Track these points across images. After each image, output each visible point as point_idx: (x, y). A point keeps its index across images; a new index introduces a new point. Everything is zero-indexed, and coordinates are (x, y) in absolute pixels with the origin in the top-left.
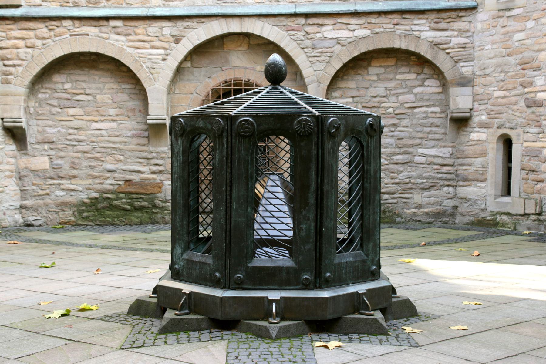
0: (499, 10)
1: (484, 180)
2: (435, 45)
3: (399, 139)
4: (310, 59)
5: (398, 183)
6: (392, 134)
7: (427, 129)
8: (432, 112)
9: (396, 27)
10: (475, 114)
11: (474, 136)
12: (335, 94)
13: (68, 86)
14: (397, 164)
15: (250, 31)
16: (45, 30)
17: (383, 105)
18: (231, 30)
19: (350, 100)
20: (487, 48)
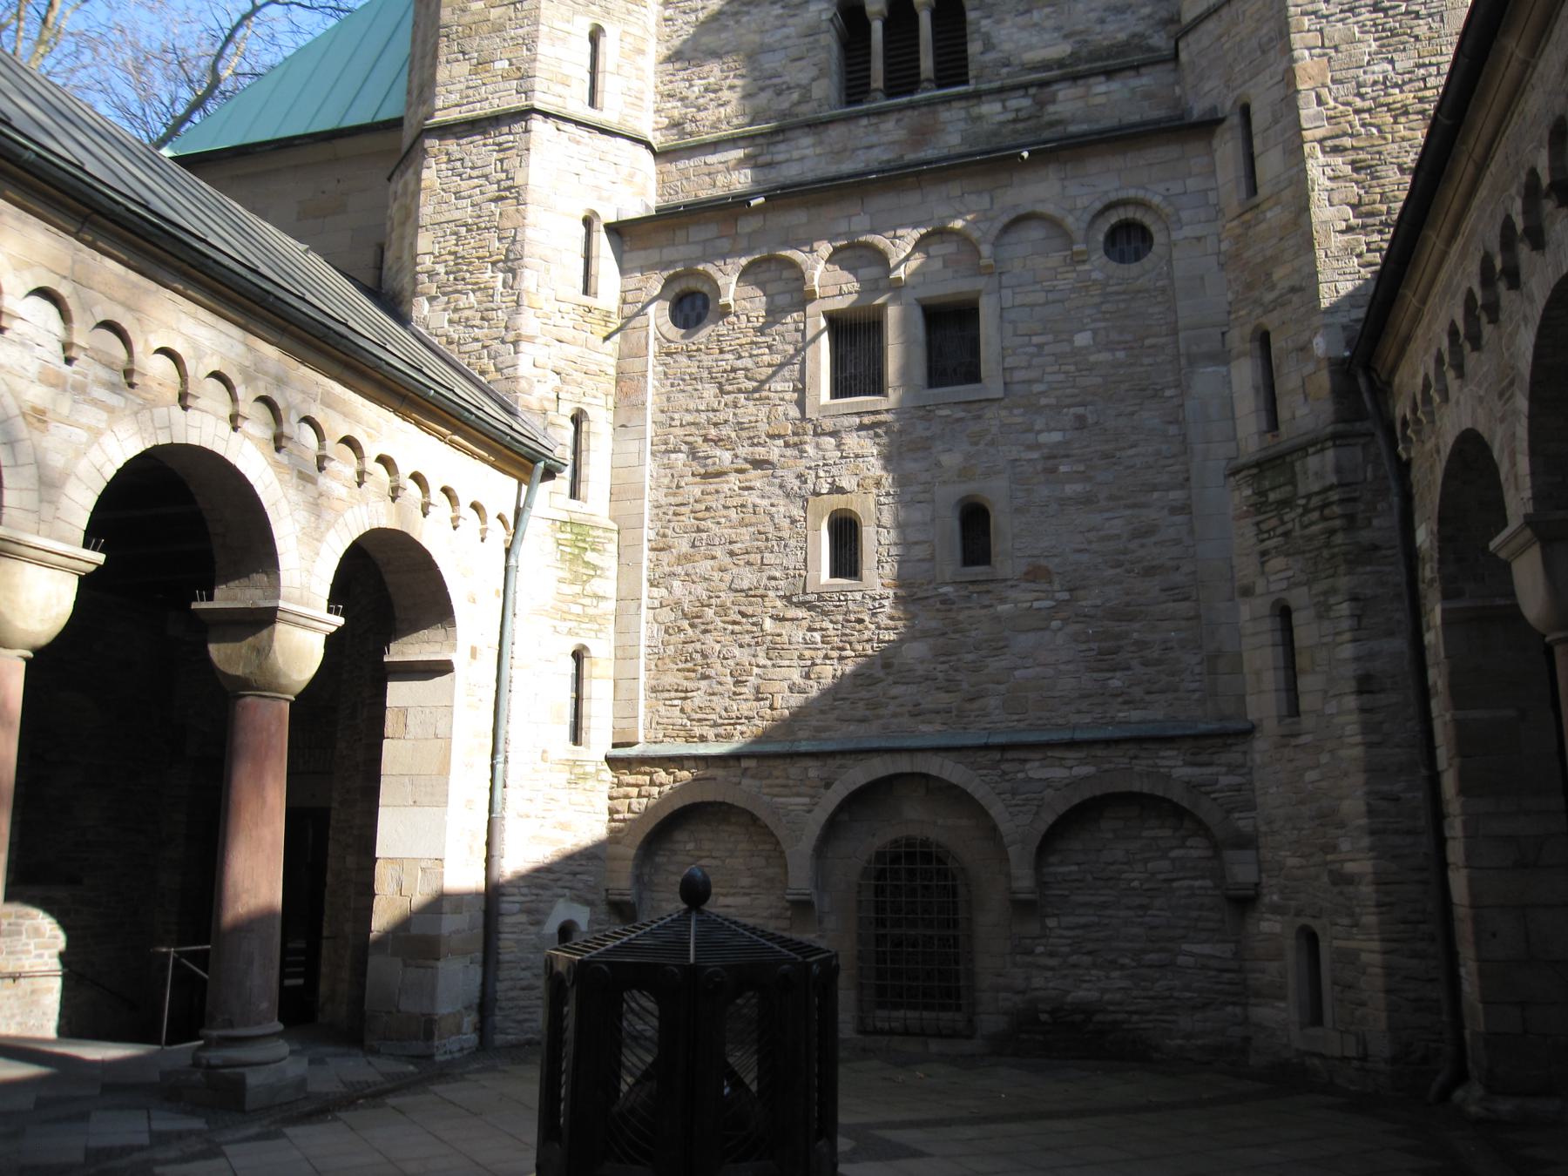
0: (1283, 736)
1: (1283, 998)
2: (1194, 787)
3: (1152, 928)
4: (1011, 809)
5: (1152, 998)
6: (1140, 920)
7: (1194, 914)
8: (1201, 888)
9: (1134, 761)
10: (1265, 891)
11: (1265, 926)
12: (1053, 859)
13: (690, 846)
14: (1150, 966)
15: (924, 771)
16: (663, 774)
17: (1124, 876)
18: (899, 770)
19: (1074, 868)
20: (1271, 791)
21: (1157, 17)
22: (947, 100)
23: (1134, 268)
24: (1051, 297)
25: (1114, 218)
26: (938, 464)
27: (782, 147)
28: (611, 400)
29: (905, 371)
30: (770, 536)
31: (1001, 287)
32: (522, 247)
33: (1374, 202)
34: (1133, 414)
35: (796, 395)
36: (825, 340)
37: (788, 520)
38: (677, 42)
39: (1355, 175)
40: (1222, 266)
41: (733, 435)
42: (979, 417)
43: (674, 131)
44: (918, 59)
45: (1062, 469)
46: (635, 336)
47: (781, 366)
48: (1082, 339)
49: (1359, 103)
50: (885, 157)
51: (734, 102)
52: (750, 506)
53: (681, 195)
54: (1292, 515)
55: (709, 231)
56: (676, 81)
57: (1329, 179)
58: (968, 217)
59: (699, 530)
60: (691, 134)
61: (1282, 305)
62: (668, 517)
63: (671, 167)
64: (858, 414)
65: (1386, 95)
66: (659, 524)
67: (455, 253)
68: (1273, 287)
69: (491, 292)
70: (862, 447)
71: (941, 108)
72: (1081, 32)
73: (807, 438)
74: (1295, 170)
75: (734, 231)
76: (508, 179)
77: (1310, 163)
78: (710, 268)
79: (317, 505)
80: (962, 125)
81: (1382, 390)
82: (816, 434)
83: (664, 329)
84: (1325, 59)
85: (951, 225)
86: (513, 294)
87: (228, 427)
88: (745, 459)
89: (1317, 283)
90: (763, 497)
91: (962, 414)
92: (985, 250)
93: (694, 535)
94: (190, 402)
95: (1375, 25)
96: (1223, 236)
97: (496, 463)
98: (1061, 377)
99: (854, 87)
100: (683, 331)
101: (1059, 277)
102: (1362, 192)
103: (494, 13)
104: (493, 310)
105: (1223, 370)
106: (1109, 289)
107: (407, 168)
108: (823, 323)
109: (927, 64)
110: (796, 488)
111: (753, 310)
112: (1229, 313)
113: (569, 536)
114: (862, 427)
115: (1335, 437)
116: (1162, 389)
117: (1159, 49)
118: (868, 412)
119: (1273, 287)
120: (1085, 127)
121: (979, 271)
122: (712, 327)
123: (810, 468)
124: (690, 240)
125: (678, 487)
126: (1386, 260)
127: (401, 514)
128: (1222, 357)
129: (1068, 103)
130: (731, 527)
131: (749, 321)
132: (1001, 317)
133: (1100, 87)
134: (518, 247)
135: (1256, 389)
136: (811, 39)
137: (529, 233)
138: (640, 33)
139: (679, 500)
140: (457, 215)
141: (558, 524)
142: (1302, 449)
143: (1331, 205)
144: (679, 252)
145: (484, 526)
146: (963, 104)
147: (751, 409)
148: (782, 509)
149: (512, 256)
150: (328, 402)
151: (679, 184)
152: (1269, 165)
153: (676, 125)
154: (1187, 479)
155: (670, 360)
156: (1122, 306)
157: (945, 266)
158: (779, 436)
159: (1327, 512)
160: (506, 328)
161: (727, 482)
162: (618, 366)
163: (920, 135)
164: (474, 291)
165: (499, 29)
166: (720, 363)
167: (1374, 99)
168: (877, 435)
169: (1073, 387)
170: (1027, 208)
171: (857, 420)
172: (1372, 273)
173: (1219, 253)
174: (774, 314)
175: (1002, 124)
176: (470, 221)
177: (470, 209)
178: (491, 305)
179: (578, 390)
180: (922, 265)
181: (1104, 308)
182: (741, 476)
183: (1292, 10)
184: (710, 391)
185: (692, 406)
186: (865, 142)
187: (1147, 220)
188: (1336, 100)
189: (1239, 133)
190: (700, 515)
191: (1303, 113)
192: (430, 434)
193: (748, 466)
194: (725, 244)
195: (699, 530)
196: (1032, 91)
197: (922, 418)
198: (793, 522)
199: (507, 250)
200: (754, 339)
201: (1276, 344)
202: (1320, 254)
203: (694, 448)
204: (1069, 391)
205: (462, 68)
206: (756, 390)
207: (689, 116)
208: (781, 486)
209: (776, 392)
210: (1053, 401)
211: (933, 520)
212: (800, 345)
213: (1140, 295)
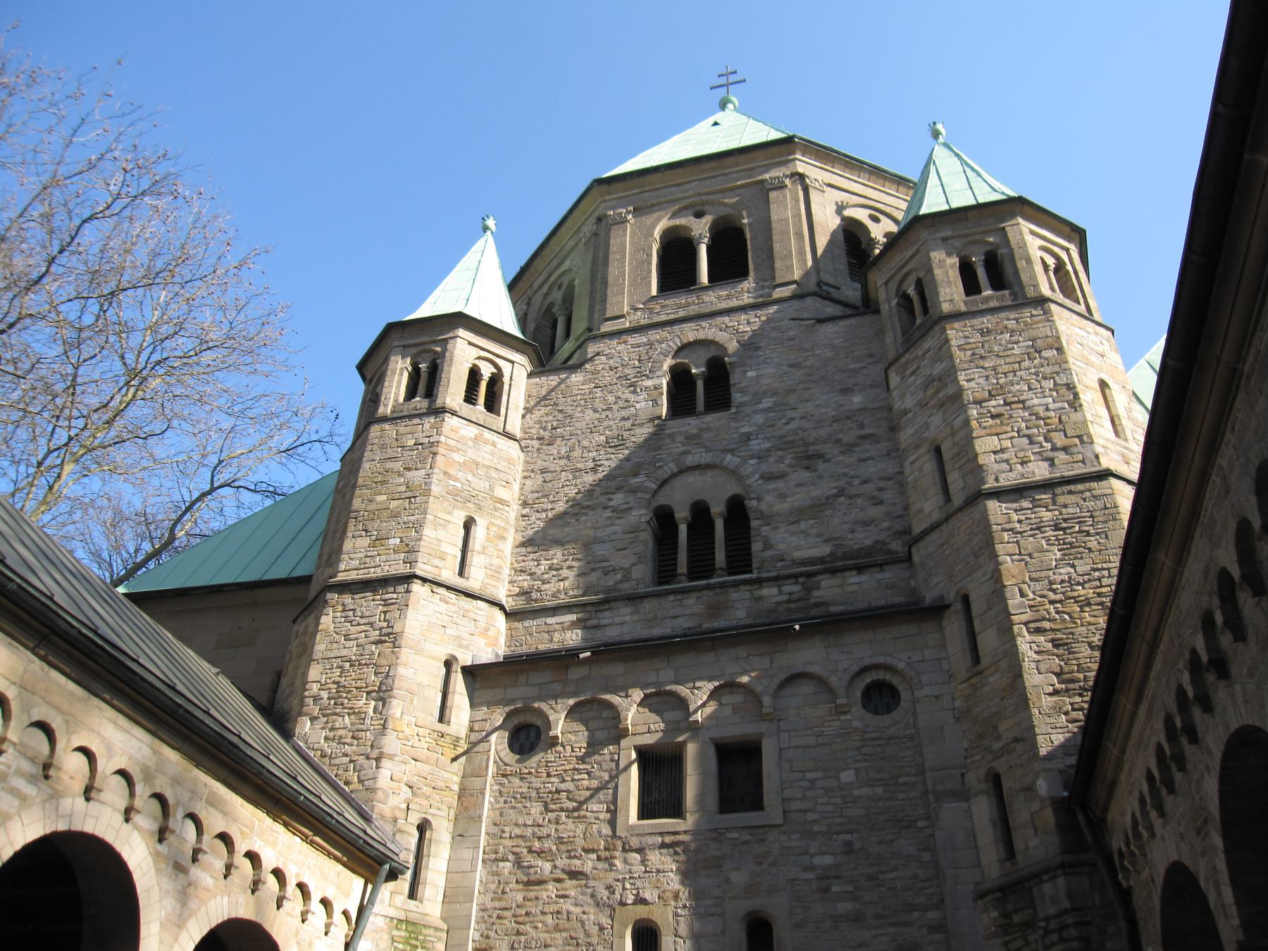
22: (736, 584)
23: (887, 719)
24: (820, 740)
25: (868, 678)
26: (728, 881)
27: (607, 614)
29: (701, 799)
30: (580, 941)
31: (779, 731)
32: (393, 681)
33: (1073, 672)
34: (892, 841)
35: (609, 815)
36: (634, 769)
37: (597, 928)
38: (530, 532)
39: (1055, 651)
40: (957, 719)
41: (554, 848)
42: (762, 840)
43: (523, 598)
44: (714, 553)
45: (835, 888)
46: (478, 759)
47: (598, 790)
48: (847, 776)
49: (1052, 596)
50: (687, 625)
51: (571, 579)
52: (565, 912)
53: (524, 647)
54: (1036, 936)
55: (546, 676)
58: (753, 674)
59: (518, 933)
60: (536, 601)
61: (1008, 752)
62: (492, 920)
63: (519, 625)
64: (661, 834)
65: (1072, 590)
66: (484, 926)
67: (338, 683)
68: (999, 738)
69: (363, 715)
70: (663, 863)
71: (731, 590)
72: (836, 539)
73: (617, 854)
74: (1008, 646)
76: (388, 627)
77: (1019, 641)
78: (544, 706)
79: (185, 894)
80: (747, 603)
81: (1099, 826)
82: (624, 850)
83: (502, 754)
84: (1023, 563)
85: (739, 680)
86: (381, 719)
87: (121, 818)
88: (563, 870)
89: (1035, 735)
90: (576, 905)
91: (747, 837)
92: (767, 700)
93: (514, 937)
94: (93, 794)
95: (1057, 540)
96: (956, 696)
97: (349, 864)
98: (831, 808)
99: (664, 571)
100: (518, 757)
101: (826, 724)
102: (1062, 663)
103: (394, 504)
105: (965, 805)
106: (867, 736)
107: (309, 615)
108: (634, 755)
109: (720, 557)
110: (605, 898)
111: (577, 742)
112: (966, 758)
113: (403, 934)
114: (663, 846)
115: (1063, 866)
116: (915, 821)
117: (897, 553)
118: (669, 833)
119: (999, 738)
120: (842, 608)
121: (762, 717)
122: (542, 754)
123: (618, 880)
124: (530, 683)
125: (503, 892)
126: (1088, 717)
127: (259, 908)
128: (963, 794)
129: (829, 590)
130: (546, 932)
131: (573, 751)
132: (780, 756)
133: (853, 579)
134: (390, 680)
135: (994, 822)
136: (633, 535)
137: (401, 670)
138: (503, 524)
139: (503, 904)
140: (344, 652)
141: (395, 921)
142: (1037, 876)
144: (520, 692)
145: (329, 921)
146: (749, 587)
147: (571, 826)
148: (592, 917)
149: (384, 688)
150: (213, 802)
152: (988, 641)
153: (524, 593)
154: (942, 901)
156: (878, 749)
157: (734, 713)
158: (593, 851)
159: (1065, 934)
160: (372, 746)
161: (546, 890)
162: (461, 784)
163: (715, 610)
164: (349, 714)
167: (1063, 593)
168: (676, 853)
169: (841, 817)
170: (800, 669)
171: (660, 840)
172: (1077, 727)
173: (953, 709)
174: (594, 746)
175: (778, 603)
176: (354, 658)
177: (355, 648)
178: (362, 726)
179: (426, 803)
180: (715, 711)
181: (864, 750)
182: (558, 885)
184: (536, 809)
185: (520, 821)
186: (673, 613)
187: (895, 681)
188: (1034, 593)
190: (520, 919)
191: (1010, 602)
192: (294, 834)
193: (565, 876)
194: (557, 687)
195: (518, 933)
196: (801, 580)
197: (715, 839)
198: (602, 929)
199: (381, 683)
201: (1007, 785)
202: (1035, 711)
203: (520, 858)
204: (837, 820)
206: (575, 809)
207: (536, 587)
208: (592, 896)
209: (592, 812)
210: (824, 828)
211: (723, 932)
212: (614, 773)
213: (892, 741)
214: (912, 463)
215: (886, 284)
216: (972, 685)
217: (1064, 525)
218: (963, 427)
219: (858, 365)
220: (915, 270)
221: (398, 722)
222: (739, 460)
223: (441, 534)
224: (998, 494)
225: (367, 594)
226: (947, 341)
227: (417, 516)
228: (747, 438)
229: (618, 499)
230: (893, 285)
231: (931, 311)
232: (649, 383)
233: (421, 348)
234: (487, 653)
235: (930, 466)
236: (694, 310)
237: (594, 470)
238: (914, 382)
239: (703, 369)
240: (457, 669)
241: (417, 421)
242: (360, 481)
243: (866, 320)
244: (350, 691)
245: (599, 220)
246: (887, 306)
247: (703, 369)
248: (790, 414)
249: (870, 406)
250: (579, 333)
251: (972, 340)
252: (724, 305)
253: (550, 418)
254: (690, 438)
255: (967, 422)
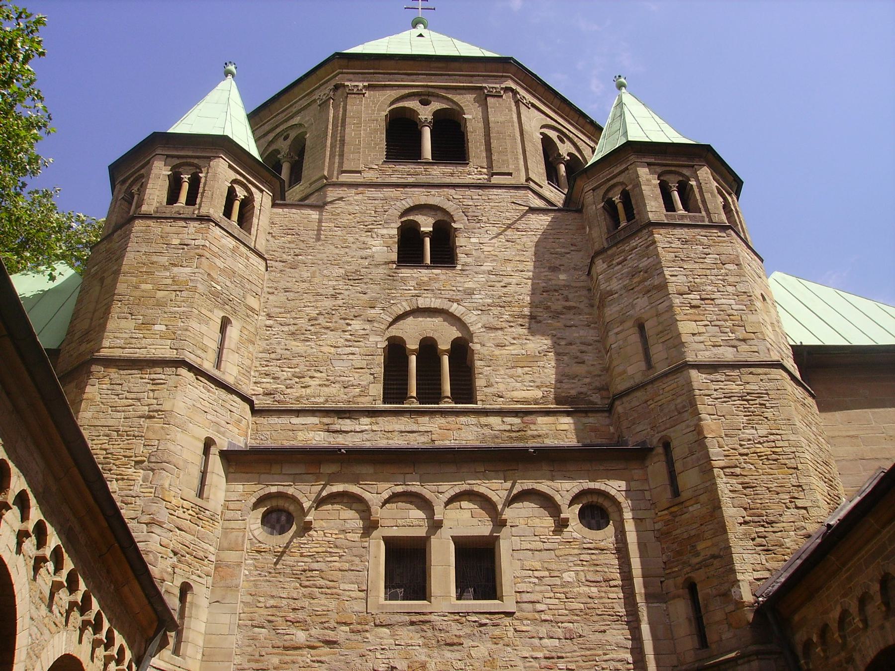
21: (594, 385)
26: (470, 656)
28: (210, 580)
48: (568, 577)
56: (272, 366)
57: (730, 491)
61: (707, 566)
68: (697, 554)
74: (708, 484)
75: (318, 471)
77: (718, 481)
86: (152, 488)
102: (749, 501)
103: (160, 294)
104: (132, 497)
114: (412, 623)
115: (757, 653)
119: (697, 554)
140: (111, 422)
143: (734, 507)
151: (269, 434)
152: (689, 479)
155: (259, 556)
156: (594, 557)
158: (345, 624)
161: (302, 655)
164: (117, 480)
165: (160, 304)
166: (300, 564)
176: (121, 428)
179: (187, 568)
181: (582, 557)
182: (312, 651)
183: (697, 392)
187: (606, 504)
189: (663, 458)
200: (328, 549)
201: (703, 592)
202: (730, 535)
205: (130, 324)
214: (617, 334)
215: (594, 190)
216: (671, 513)
217: (748, 397)
218: (667, 311)
219: (563, 250)
220: (622, 183)
221: (167, 493)
222: (464, 309)
223: (204, 329)
224: (701, 367)
225: (133, 371)
226: (654, 242)
227: (183, 309)
228: (470, 293)
229: (356, 325)
230: (601, 192)
231: (637, 217)
232: (384, 232)
233: (184, 160)
234: (239, 442)
235: (635, 338)
236: (422, 179)
237: (334, 296)
238: (621, 270)
239: (431, 229)
240: (214, 450)
241: (183, 223)
242: (124, 268)
243: (570, 216)
244: (118, 459)
245: (337, 87)
246: (594, 207)
247: (431, 229)
248: (506, 280)
249: (574, 284)
250: (314, 179)
251: (673, 245)
252: (448, 180)
253: (293, 246)
254: (420, 285)
255: (671, 307)
